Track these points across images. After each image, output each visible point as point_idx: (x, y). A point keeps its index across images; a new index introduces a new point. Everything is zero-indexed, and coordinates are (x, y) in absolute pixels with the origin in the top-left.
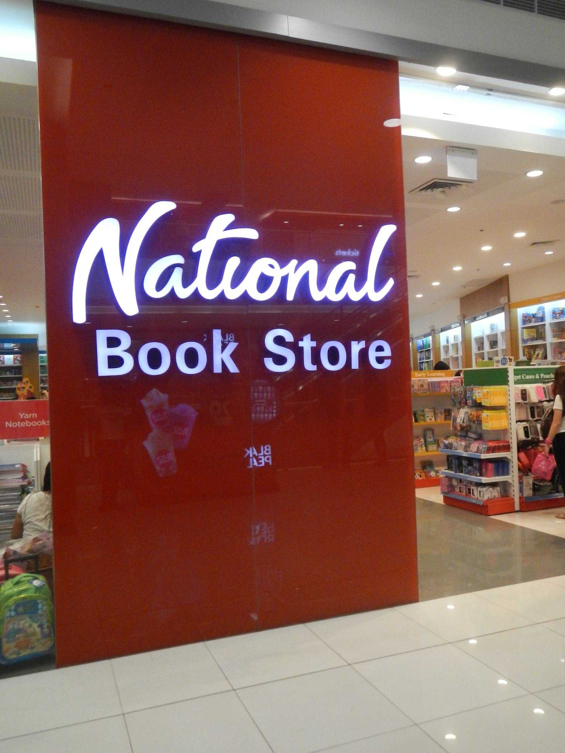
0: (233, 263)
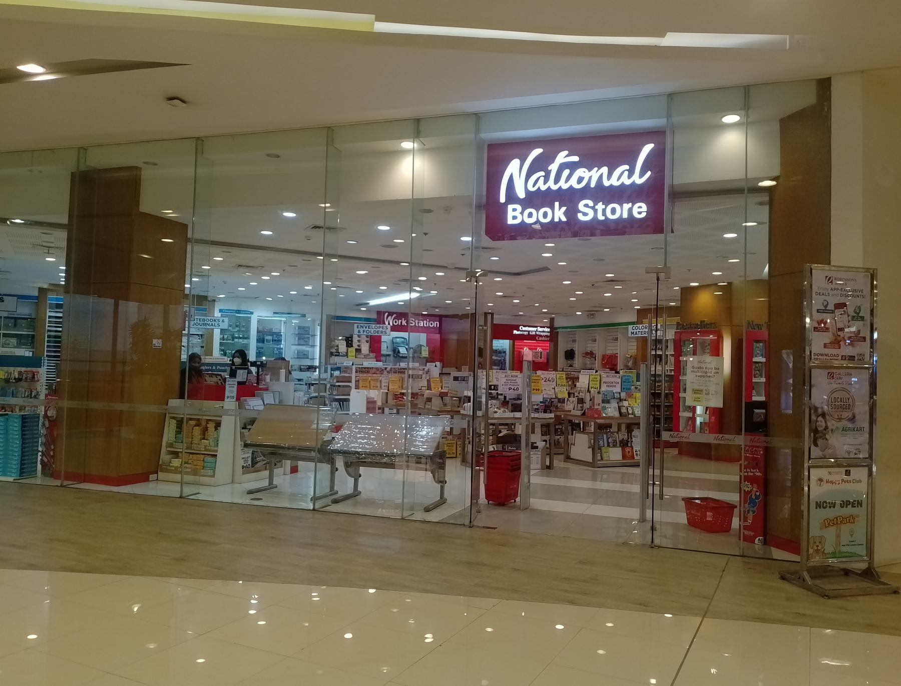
0: (566, 172)
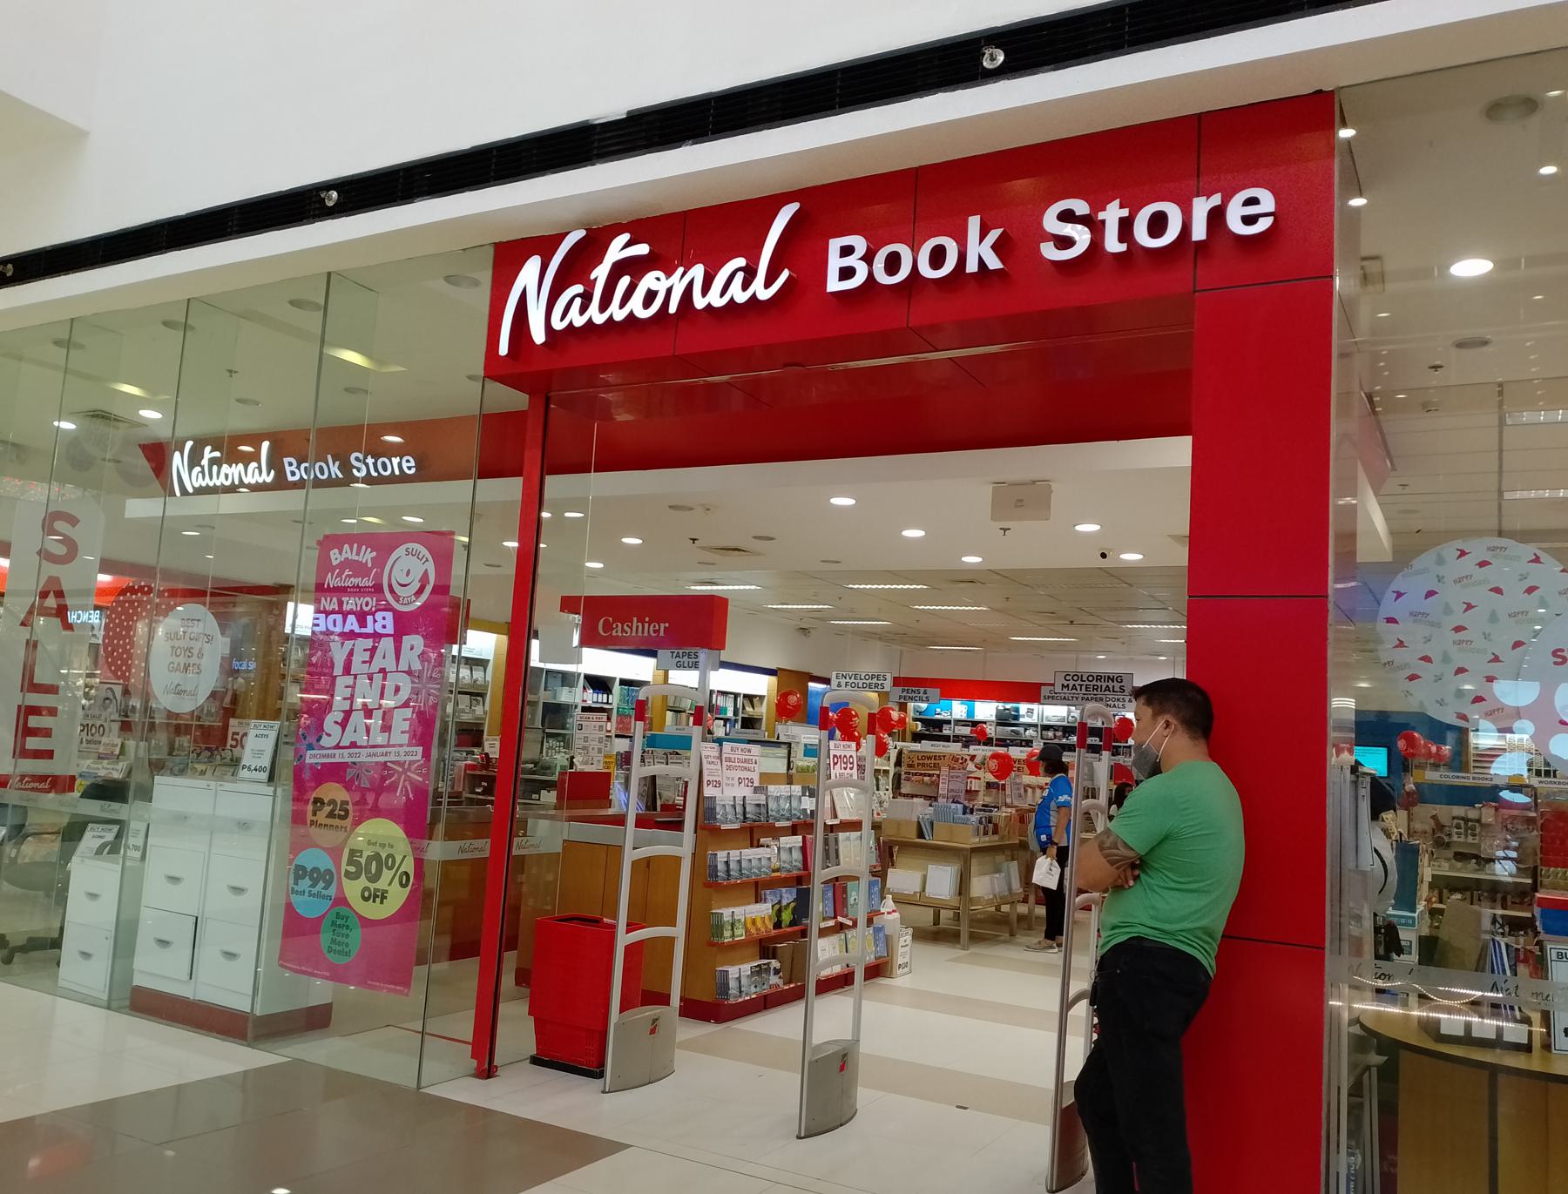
0: (625, 282)
